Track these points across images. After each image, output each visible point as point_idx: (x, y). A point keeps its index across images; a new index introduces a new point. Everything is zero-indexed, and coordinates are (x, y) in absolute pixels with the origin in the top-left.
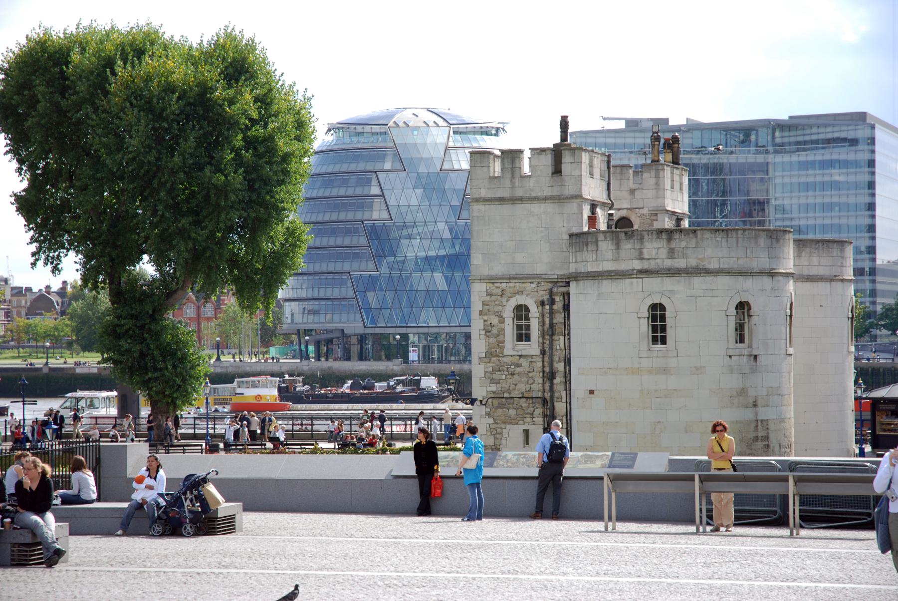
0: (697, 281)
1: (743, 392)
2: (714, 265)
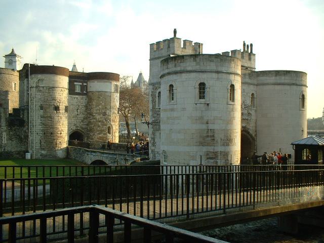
0: (184, 75)
1: (201, 118)
2: (189, 68)
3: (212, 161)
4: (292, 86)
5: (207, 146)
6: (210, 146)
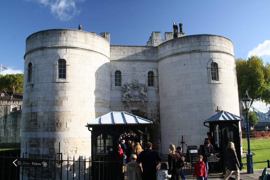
3: (34, 149)
4: (193, 54)
5: (31, 131)
6: (34, 131)
